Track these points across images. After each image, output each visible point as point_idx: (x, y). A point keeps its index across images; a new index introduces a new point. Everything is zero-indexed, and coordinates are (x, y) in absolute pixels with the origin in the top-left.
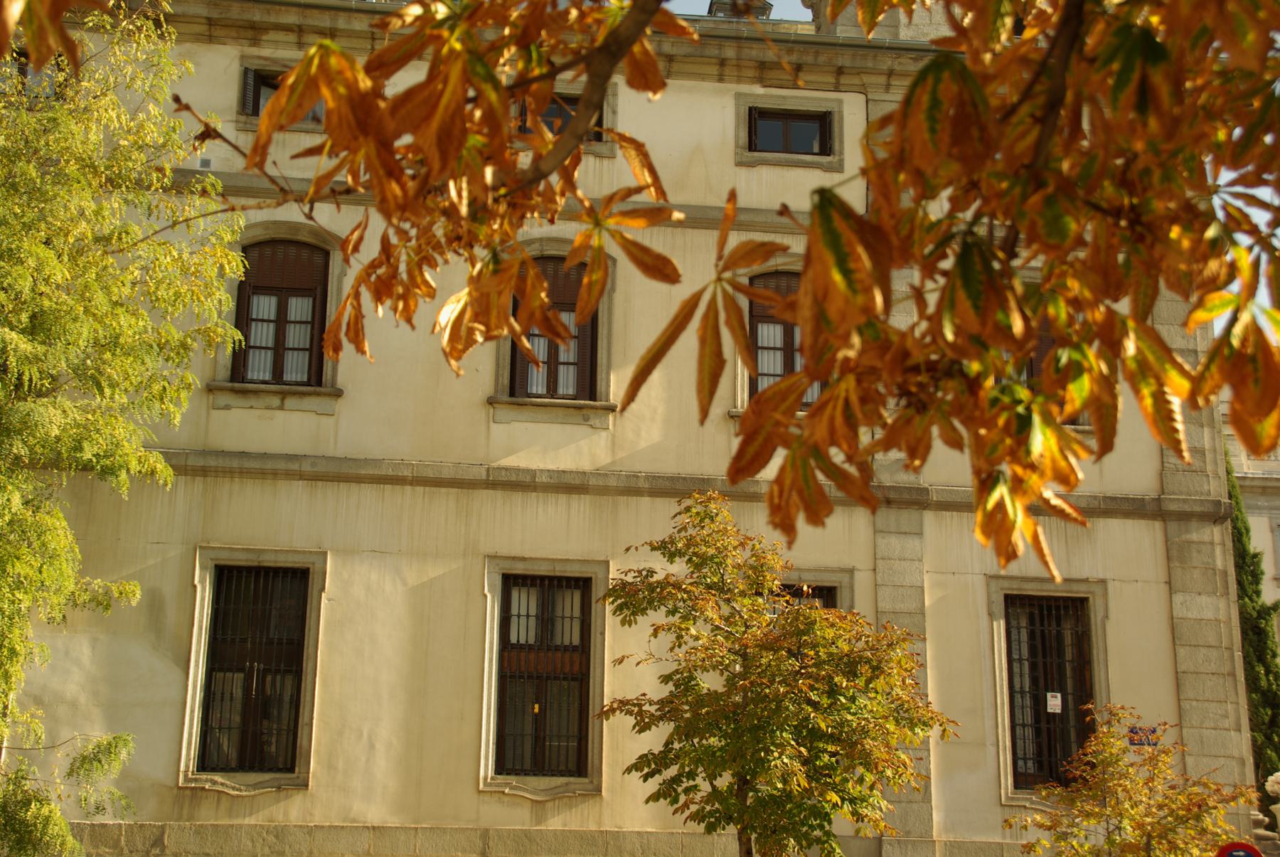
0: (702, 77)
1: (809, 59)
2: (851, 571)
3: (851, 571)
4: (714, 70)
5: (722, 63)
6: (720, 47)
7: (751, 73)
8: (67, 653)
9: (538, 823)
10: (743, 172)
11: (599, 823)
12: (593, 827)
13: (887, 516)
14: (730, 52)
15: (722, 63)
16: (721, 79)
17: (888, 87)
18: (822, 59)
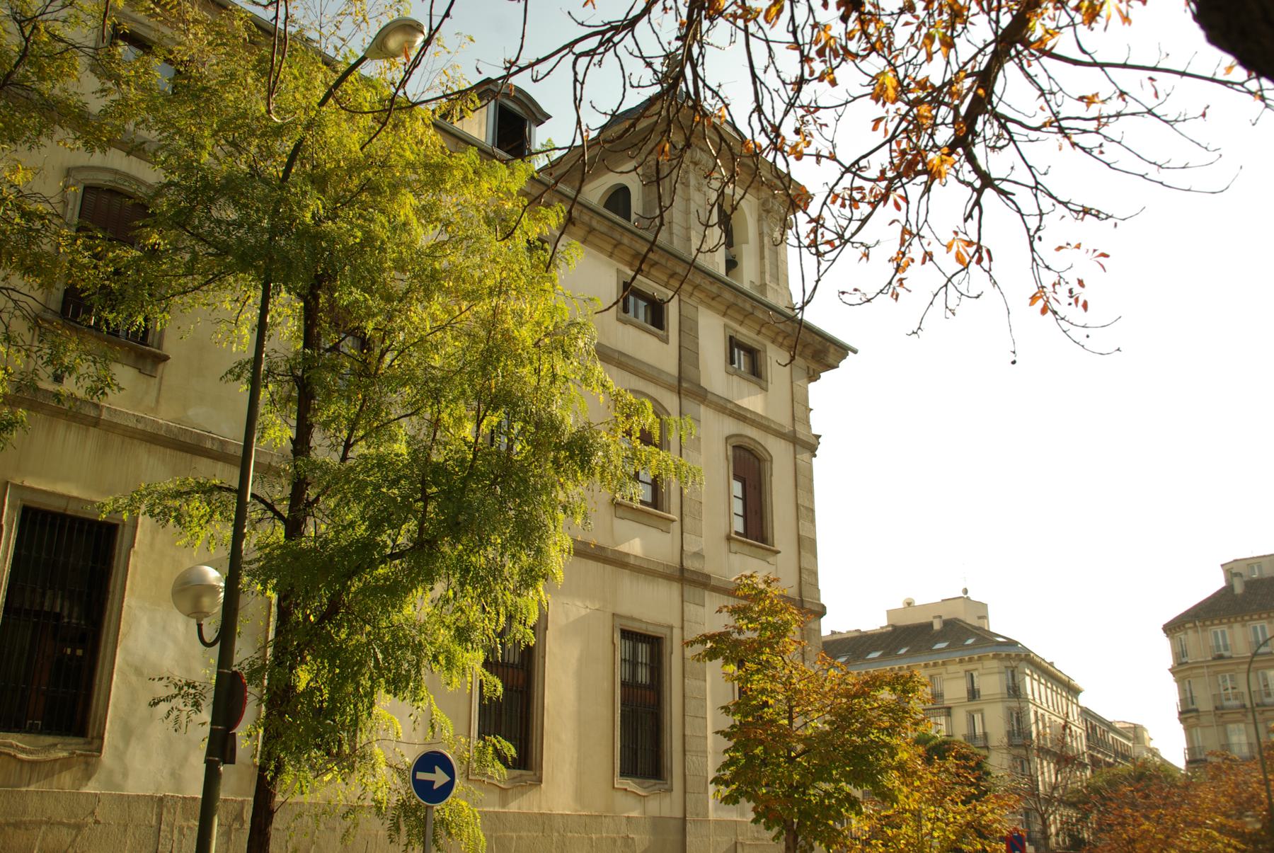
0: (601, 250)
1: (663, 261)
2: (671, 628)
3: (671, 628)
4: (609, 248)
5: (618, 244)
6: (622, 235)
7: (628, 258)
8: (164, 628)
9: (504, 806)
10: (620, 325)
11: (540, 808)
12: (536, 811)
13: (689, 590)
14: (626, 241)
15: (618, 244)
16: (611, 256)
17: (691, 295)
18: (669, 264)
